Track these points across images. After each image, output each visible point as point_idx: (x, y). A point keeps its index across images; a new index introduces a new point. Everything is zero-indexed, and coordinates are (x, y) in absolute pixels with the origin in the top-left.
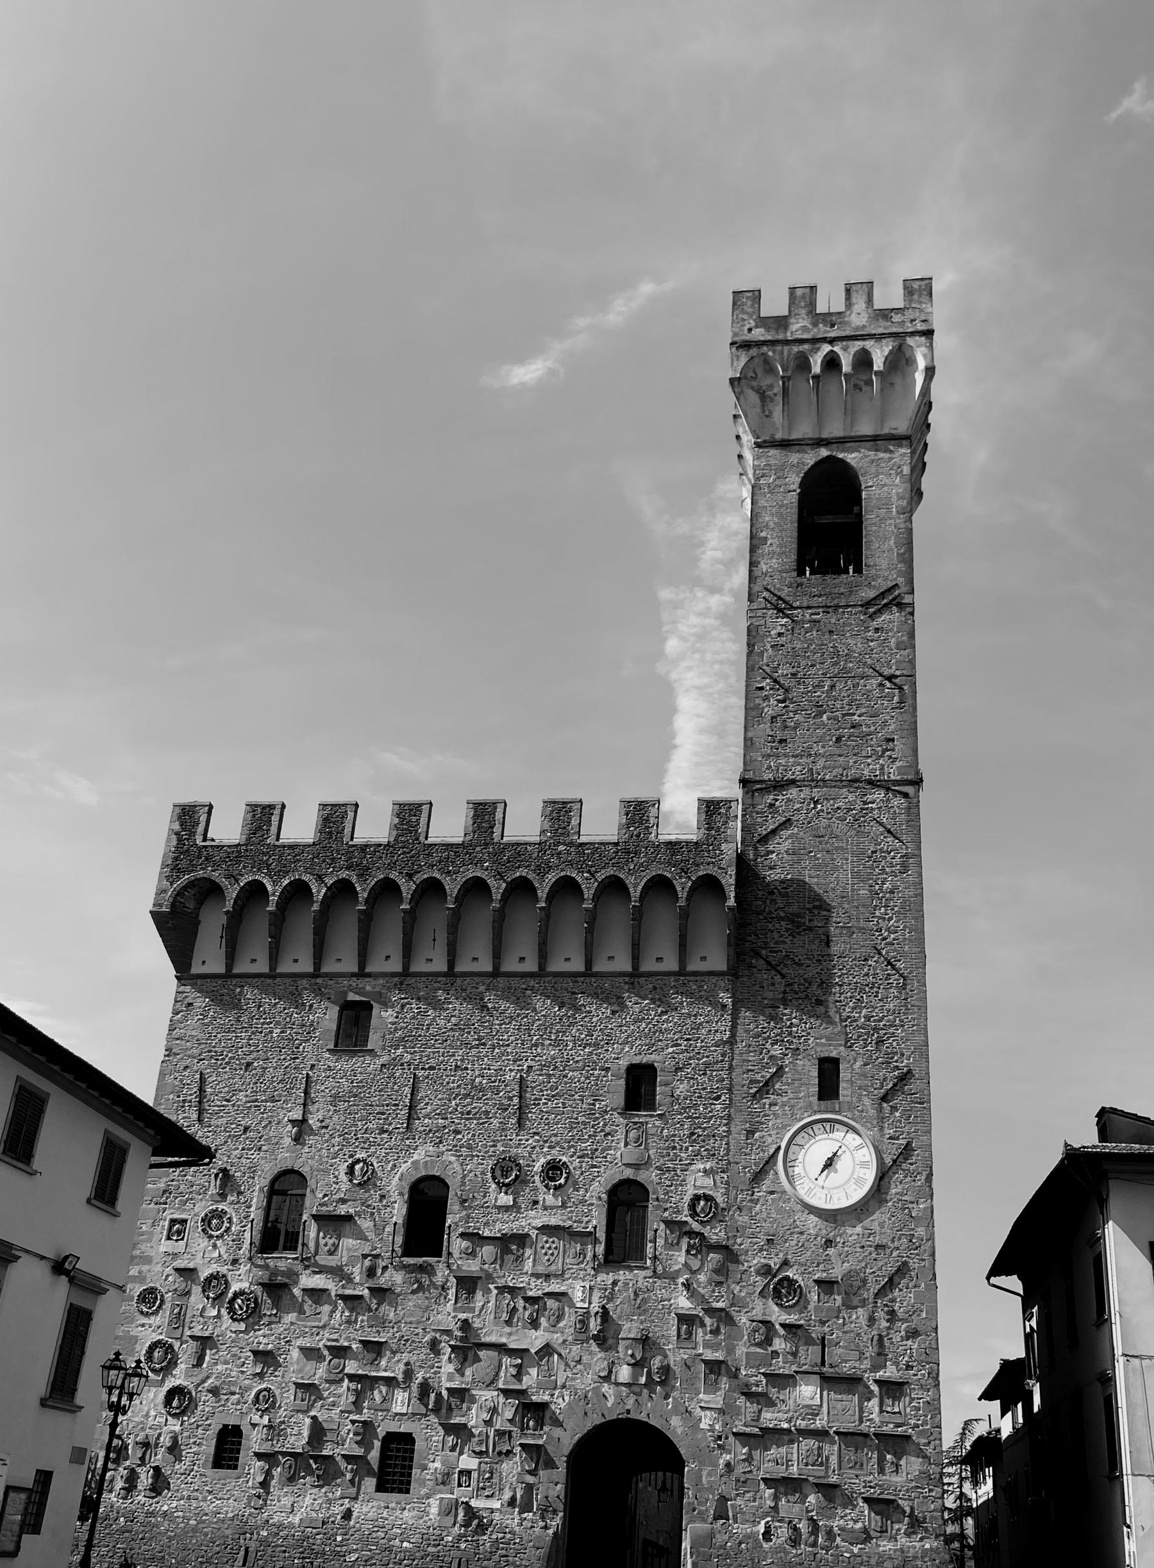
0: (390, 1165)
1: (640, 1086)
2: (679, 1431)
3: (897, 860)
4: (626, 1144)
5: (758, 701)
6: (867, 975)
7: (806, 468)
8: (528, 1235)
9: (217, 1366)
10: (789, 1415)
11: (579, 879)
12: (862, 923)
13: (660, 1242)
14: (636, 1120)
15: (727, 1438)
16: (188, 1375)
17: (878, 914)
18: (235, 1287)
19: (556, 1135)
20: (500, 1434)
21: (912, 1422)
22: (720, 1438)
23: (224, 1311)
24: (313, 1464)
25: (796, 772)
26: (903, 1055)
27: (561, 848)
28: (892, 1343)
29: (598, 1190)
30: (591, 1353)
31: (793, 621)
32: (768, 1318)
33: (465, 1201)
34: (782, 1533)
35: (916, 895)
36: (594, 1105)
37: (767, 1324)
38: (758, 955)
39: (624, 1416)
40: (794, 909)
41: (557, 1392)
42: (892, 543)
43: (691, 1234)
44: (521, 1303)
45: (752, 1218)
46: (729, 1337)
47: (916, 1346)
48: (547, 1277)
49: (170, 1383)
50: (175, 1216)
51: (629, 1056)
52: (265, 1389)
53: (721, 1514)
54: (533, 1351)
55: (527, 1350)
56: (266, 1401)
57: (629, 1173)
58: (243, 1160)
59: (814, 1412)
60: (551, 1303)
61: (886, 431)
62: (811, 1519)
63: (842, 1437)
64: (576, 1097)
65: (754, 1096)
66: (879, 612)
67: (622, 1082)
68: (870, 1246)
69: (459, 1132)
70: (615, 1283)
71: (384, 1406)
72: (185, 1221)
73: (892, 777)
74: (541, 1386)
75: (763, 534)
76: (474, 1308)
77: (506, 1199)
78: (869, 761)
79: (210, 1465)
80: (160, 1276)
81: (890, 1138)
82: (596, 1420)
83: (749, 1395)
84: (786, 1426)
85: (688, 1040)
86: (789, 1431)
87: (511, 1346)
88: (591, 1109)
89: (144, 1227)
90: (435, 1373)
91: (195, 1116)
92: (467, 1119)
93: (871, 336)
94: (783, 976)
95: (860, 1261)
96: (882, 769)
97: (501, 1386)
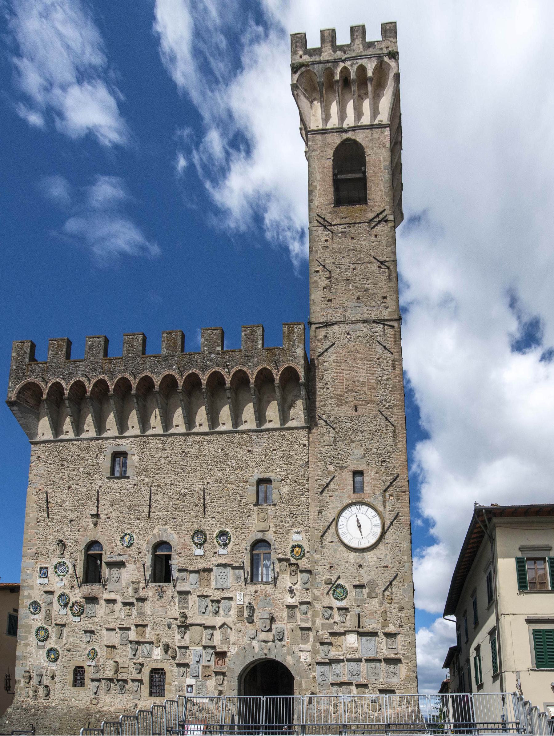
3: (390, 363)
4: (258, 520)
5: (315, 278)
6: (376, 426)
7: (336, 146)
9: (69, 637)
10: (343, 652)
12: (373, 398)
14: (263, 508)
16: (56, 642)
17: (381, 393)
18: (73, 600)
19: (223, 518)
20: (204, 667)
21: (402, 652)
23: (69, 612)
24: (117, 681)
25: (337, 317)
26: (395, 467)
28: (392, 615)
29: (246, 545)
31: (332, 232)
32: (330, 605)
35: (399, 382)
37: (331, 608)
38: (321, 419)
39: (264, 657)
40: (338, 392)
44: (210, 604)
46: (313, 616)
47: (403, 615)
49: (48, 647)
50: (42, 566)
51: (258, 474)
52: (93, 649)
54: (217, 627)
56: (93, 654)
57: (260, 536)
58: (71, 536)
59: (356, 650)
61: (376, 122)
64: (232, 497)
68: (380, 567)
69: (175, 519)
70: (256, 592)
71: (149, 656)
72: (47, 568)
73: (386, 318)
75: (315, 184)
77: (200, 552)
78: (374, 309)
79: (72, 685)
80: (37, 595)
82: (249, 660)
84: (341, 658)
85: (287, 464)
87: (206, 625)
88: (240, 503)
89: (28, 571)
91: (46, 515)
92: (179, 511)
94: (334, 429)
96: (381, 313)
97: (203, 644)
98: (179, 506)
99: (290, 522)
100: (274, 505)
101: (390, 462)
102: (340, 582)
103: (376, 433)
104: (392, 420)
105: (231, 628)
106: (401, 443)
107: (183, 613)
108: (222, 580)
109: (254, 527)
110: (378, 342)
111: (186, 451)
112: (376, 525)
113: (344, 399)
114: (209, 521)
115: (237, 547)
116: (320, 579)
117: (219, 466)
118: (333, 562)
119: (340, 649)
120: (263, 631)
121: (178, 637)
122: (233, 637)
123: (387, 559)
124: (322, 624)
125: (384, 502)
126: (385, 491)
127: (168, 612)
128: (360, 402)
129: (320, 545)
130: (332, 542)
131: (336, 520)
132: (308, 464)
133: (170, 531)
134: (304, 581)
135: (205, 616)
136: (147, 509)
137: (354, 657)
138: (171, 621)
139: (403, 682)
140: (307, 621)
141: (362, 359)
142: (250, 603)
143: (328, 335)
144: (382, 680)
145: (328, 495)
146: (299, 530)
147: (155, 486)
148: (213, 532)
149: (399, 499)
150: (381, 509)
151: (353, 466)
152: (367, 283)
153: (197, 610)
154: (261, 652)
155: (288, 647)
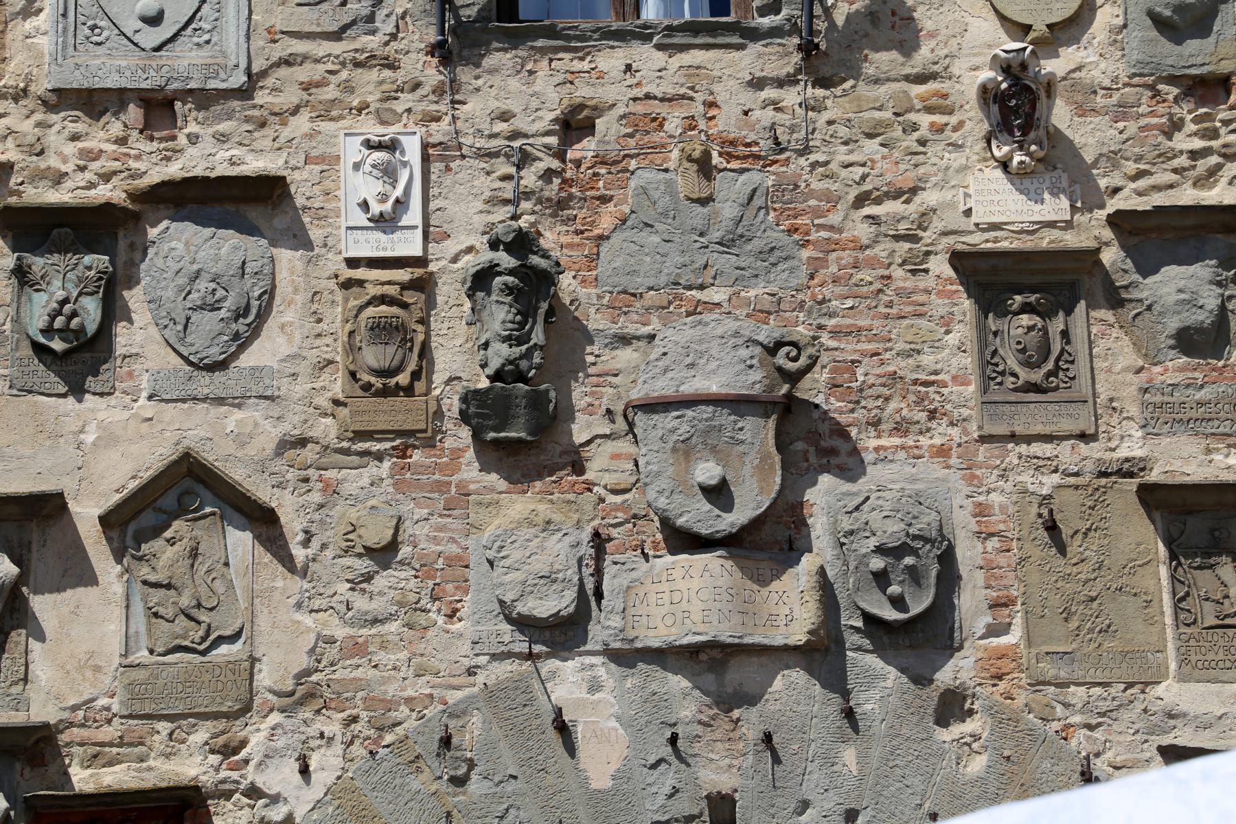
48: (159, 108)
54: (86, 515)
55: (47, 508)
60: (176, 244)
70: (575, 125)
74: (148, 712)
105: (263, 521)
120: (684, 541)
122: (283, 627)
142: (522, 244)
154: (667, 778)
155: (1003, 719)
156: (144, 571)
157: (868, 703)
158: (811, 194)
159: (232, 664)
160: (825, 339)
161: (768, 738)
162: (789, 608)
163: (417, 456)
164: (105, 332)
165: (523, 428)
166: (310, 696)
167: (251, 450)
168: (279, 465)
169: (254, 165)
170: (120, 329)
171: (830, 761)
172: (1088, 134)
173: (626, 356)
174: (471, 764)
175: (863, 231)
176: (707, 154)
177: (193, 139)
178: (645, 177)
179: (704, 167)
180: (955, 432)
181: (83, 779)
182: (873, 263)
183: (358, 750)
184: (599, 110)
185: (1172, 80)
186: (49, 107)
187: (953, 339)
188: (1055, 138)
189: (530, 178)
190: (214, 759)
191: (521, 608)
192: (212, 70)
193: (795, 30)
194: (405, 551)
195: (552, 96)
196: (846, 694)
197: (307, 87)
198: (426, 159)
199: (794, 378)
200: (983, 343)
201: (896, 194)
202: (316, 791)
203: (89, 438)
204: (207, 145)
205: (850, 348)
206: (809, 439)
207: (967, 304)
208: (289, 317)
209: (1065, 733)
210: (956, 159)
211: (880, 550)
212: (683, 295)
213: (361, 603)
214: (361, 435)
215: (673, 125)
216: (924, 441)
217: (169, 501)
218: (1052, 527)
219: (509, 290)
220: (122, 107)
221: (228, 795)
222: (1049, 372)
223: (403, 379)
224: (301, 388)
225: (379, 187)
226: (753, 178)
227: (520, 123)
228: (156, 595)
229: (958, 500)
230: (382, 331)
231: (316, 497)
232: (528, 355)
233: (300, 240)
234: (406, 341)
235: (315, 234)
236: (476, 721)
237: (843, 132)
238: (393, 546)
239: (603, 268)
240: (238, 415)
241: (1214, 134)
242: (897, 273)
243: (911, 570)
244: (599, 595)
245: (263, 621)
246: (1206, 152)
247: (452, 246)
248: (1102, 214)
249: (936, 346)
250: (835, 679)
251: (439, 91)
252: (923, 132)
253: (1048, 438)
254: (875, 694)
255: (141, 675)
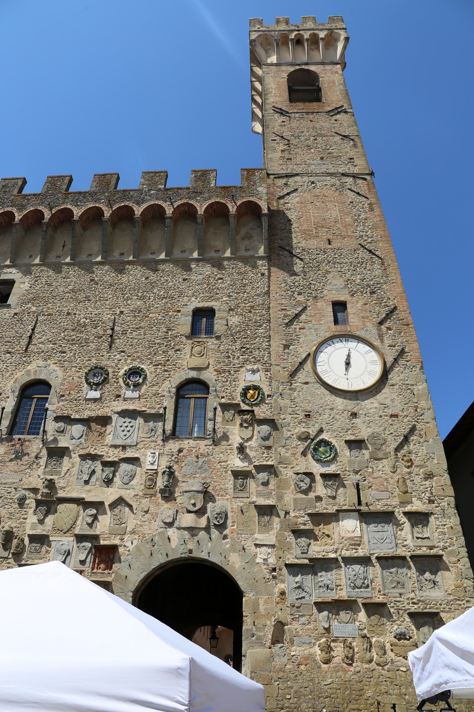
0: (9, 374)
1: (203, 318)
2: (237, 566)
3: (366, 205)
8: (110, 418)
10: (335, 547)
11: (164, 205)
13: (219, 419)
14: (200, 340)
15: (280, 569)
19: (137, 352)
21: (441, 544)
22: (274, 570)
26: (389, 299)
27: (152, 192)
29: (169, 386)
30: (158, 505)
31: (289, 117)
32: (308, 471)
33: (63, 396)
34: (339, 651)
36: (167, 332)
37: (310, 475)
41: (126, 537)
42: (338, 93)
43: (242, 412)
44: (98, 466)
45: (292, 401)
48: (124, 448)
53: (278, 636)
54: (107, 504)
55: (102, 503)
57: (193, 374)
59: (357, 543)
60: (124, 467)
62: (364, 637)
63: (383, 562)
64: (154, 328)
65: (287, 324)
66: (336, 114)
67: (190, 318)
68: (386, 416)
70: (180, 451)
74: (113, 533)
76: (60, 472)
77: (95, 394)
78: (341, 166)
81: (389, 346)
83: (297, 533)
84: (332, 555)
85: (237, 293)
86: (336, 559)
87: (86, 500)
90: (21, 523)
93: (318, 29)
94: (301, 260)
95: (380, 426)
97: (77, 532)
98: (74, 337)
99: (241, 357)
100: (218, 338)
101: (382, 293)
102: (324, 436)
103: (359, 265)
104: (377, 253)
105: (130, 507)
106: (393, 274)
107: (52, 480)
108: (124, 433)
109: (185, 363)
110: (349, 189)
111: (96, 279)
112: (373, 362)
113: (313, 234)
114: (116, 356)
115: (155, 388)
116: (289, 433)
117: (140, 294)
118: (309, 409)
119: (329, 541)
121: (32, 519)
122: (131, 521)
123: (394, 404)
124: (295, 500)
125: (381, 337)
126: (381, 323)
127: (24, 480)
128: (335, 237)
129: (288, 387)
130: (307, 383)
131: (312, 356)
132: (268, 293)
133: (53, 367)
134: (262, 435)
135: (88, 487)
136: (26, 341)
137: (356, 555)
138: (27, 493)
139: (452, 597)
140: (268, 495)
141: (332, 201)
142: (170, 468)
143: (289, 183)
144: (412, 595)
145: (298, 327)
146: (255, 367)
147: (43, 315)
148: (119, 369)
149: (401, 332)
150: (377, 343)
151: (332, 296)
152: (331, 148)
153: (75, 477)
154: (183, 547)
155: (233, 539)
156: (114, 513)
157: (213, 536)
158: (212, 461)
159: (124, 527)
160: (212, 482)
161: (198, 541)
162: (203, 522)
163: (153, 498)
164: (113, 478)
165: (168, 494)
166: (134, 532)
167: (130, 496)
168: (134, 498)
169: (136, 456)
170: (115, 478)
171: (207, 545)
172: (251, 454)
173: (184, 484)
174: (155, 543)
175: (219, 467)
176: (198, 455)
177: (128, 452)
178: (189, 458)
179: (197, 457)
180: (229, 496)
181: (102, 543)
182: (220, 472)
183: (140, 541)
184: (184, 449)
185: (263, 446)
186: (110, 447)
187: (230, 483)
188: (247, 454)
189: (173, 458)
190: (120, 541)
191: (165, 521)
192: (132, 442)
193: (212, 438)
194: (150, 512)
195: (178, 447)
196: (210, 535)
197: (144, 445)
198: (159, 455)
199: (207, 488)
200: (234, 484)
201: (224, 462)
202: (133, 546)
203: (109, 494)
204: (130, 453)
205: (216, 484)
206: (207, 496)
207: (233, 478)
208: (137, 477)
209: (241, 541)
210: (233, 457)
211: (216, 514)
212: (193, 475)
213: (143, 519)
214: (145, 495)
215: (194, 451)
216: (225, 498)
217: (118, 503)
218: (242, 511)
219: (167, 474)
220: (119, 447)
221: (121, 546)
222: (243, 488)
223: (152, 487)
224: (138, 487)
225: (152, 459)
226: (204, 459)
227: (172, 450)
228: (115, 516)
229: (229, 506)
230: (150, 479)
231: (138, 503)
232: (169, 484)
233: (140, 466)
234: (153, 481)
235: (143, 465)
236: (157, 537)
237: (218, 453)
238: (148, 511)
239: (182, 471)
240: (129, 491)
241: (269, 454)
242: (223, 473)
243: (221, 517)
244: (176, 519)
245: (129, 521)
246: (268, 457)
247: (161, 468)
248: (252, 465)
249: (228, 484)
250: (209, 533)
251: (162, 446)
252: (229, 453)
253: (242, 498)
254: (214, 535)
255: (111, 528)
